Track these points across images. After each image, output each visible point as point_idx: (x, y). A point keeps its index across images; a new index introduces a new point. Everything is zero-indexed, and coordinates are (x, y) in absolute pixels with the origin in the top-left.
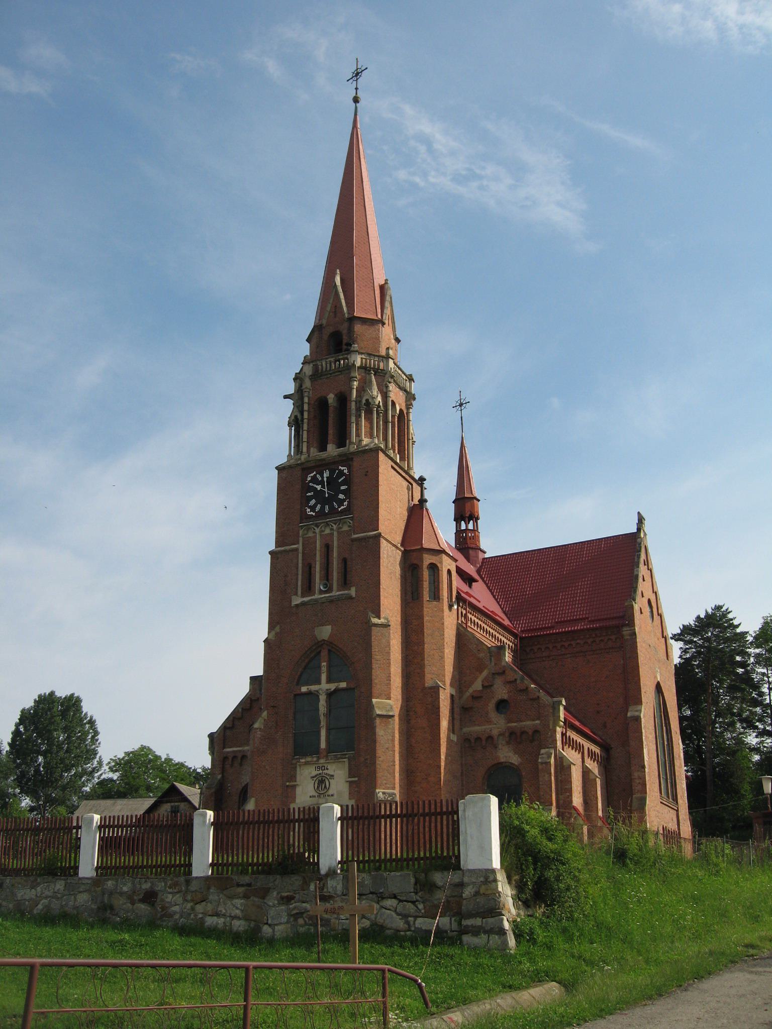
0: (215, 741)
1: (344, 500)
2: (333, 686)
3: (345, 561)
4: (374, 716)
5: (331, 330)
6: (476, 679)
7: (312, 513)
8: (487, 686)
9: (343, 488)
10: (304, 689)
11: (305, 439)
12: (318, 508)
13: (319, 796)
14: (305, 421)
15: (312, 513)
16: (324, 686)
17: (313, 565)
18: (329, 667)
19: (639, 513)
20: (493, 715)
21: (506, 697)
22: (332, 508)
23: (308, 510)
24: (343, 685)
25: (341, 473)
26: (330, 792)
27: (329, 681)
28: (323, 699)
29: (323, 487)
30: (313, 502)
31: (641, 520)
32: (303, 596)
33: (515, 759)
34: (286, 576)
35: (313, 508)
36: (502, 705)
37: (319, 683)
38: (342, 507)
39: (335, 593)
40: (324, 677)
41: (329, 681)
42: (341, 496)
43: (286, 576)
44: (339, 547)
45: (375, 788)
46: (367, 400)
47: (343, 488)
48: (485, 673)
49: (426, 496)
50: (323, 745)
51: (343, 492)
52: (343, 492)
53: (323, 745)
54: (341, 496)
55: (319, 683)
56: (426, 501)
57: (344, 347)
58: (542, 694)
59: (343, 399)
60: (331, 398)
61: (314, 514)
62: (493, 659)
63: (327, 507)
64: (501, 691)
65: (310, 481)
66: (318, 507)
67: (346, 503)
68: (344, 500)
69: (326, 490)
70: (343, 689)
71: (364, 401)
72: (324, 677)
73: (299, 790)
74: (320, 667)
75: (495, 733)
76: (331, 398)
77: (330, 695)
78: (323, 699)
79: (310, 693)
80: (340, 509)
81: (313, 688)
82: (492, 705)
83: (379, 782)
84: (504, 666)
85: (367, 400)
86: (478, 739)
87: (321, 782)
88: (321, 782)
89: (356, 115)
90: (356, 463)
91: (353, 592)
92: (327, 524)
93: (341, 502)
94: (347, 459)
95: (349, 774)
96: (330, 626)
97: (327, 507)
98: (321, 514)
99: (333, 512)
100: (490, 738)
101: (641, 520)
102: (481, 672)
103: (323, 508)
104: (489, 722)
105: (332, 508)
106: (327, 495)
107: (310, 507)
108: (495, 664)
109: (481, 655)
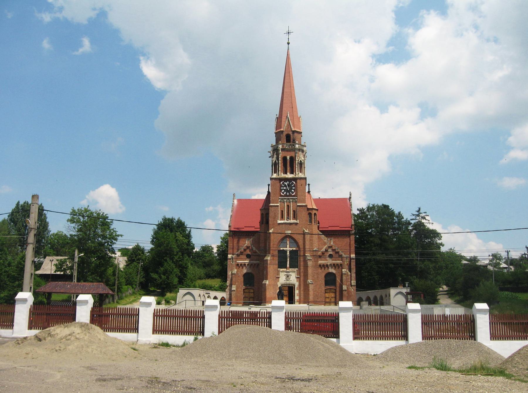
2: (291, 249)
3: (294, 211)
4: (307, 259)
5: (286, 133)
8: (326, 251)
9: (293, 188)
10: (281, 249)
11: (280, 170)
13: (287, 280)
14: (280, 164)
16: (288, 249)
17: (283, 211)
18: (290, 243)
19: (350, 192)
20: (328, 258)
22: (289, 193)
23: (281, 193)
24: (294, 249)
25: (293, 183)
26: (290, 280)
27: (290, 247)
28: (288, 252)
29: (286, 187)
30: (283, 191)
31: (350, 195)
32: (280, 220)
34: (275, 213)
35: (283, 193)
37: (287, 247)
39: (292, 221)
40: (288, 246)
41: (290, 247)
42: (293, 191)
43: (275, 213)
45: (308, 279)
46: (301, 161)
47: (293, 188)
48: (326, 246)
50: (288, 266)
51: (293, 189)
52: (293, 189)
53: (288, 266)
54: (293, 191)
55: (287, 247)
57: (292, 140)
58: (343, 254)
59: (292, 159)
60: (288, 158)
63: (288, 193)
64: (330, 252)
65: (282, 184)
67: (294, 193)
68: (294, 192)
70: (294, 250)
71: (300, 161)
72: (288, 246)
73: (280, 279)
74: (287, 243)
75: (329, 264)
76: (288, 158)
77: (290, 252)
78: (288, 252)
79: (283, 250)
81: (285, 249)
83: (309, 278)
85: (301, 161)
86: (323, 265)
87: (288, 276)
88: (288, 276)
89: (288, 49)
90: (298, 181)
91: (298, 222)
93: (293, 193)
94: (295, 179)
97: (288, 193)
98: (286, 195)
99: (290, 195)
100: (327, 265)
101: (350, 195)
103: (286, 194)
104: (326, 260)
105: (289, 193)
107: (282, 192)
109: (325, 241)
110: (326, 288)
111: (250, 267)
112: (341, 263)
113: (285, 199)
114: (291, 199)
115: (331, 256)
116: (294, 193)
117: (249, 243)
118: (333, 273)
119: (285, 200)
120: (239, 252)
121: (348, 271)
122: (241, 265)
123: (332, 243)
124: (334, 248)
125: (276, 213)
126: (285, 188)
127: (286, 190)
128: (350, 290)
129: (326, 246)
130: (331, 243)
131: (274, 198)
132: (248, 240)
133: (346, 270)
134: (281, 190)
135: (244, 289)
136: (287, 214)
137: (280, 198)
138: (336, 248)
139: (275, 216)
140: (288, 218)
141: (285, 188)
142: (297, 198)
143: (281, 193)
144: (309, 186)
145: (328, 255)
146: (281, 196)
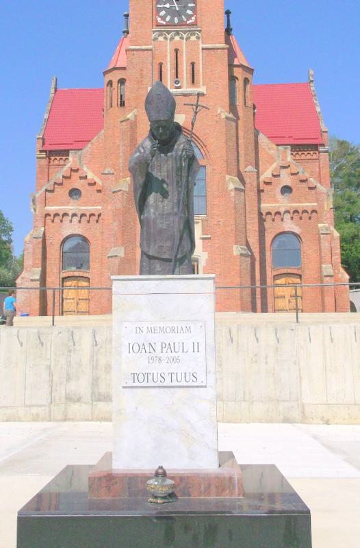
0: (37, 200)
1: (192, 16)
6: (267, 169)
7: (162, 22)
12: (168, 18)
15: (162, 22)
20: (279, 196)
21: (289, 184)
22: (181, 20)
23: (159, 19)
30: (163, 13)
33: (297, 230)
34: (141, 70)
35: (163, 18)
36: (286, 190)
38: (190, 21)
42: (189, 12)
43: (141, 70)
44: (188, 53)
48: (274, 165)
49: (231, 27)
52: (191, 9)
54: (189, 12)
56: (231, 30)
61: (164, 23)
62: (281, 156)
64: (286, 179)
66: (168, 18)
68: (192, 16)
69: (176, 5)
75: (282, 210)
80: (188, 22)
82: (278, 189)
84: (289, 162)
91: (203, 89)
92: (177, 33)
93: (189, 17)
95: (203, 232)
96: (184, 115)
99: (182, 24)
100: (278, 213)
102: (272, 163)
103: (172, 19)
104: (276, 201)
105: (181, 20)
106: (177, 9)
107: (160, 17)
108: (283, 160)
109: (272, 152)
110: (275, 273)
111: (80, 222)
112: (313, 206)
113: (168, 32)
114: (185, 32)
115: (286, 190)
116: (193, 18)
117: (77, 159)
118: (293, 233)
119: (169, 36)
120: (52, 183)
121: (332, 228)
122: (56, 215)
123: (289, 158)
124: (294, 169)
125: (144, 69)
126: (168, 6)
127: (171, 12)
128: (340, 276)
129: (274, 165)
130: (286, 157)
131: (138, 31)
132: (76, 153)
133: (327, 225)
134: (159, 10)
135: (63, 279)
136: (174, 71)
137: (154, 32)
138: (300, 170)
139: (142, 77)
140: (177, 82)
141: (168, 6)
142: (200, 31)
143: (159, 19)
144: (228, 17)
145: (282, 186)
146: (159, 25)
